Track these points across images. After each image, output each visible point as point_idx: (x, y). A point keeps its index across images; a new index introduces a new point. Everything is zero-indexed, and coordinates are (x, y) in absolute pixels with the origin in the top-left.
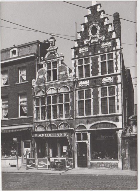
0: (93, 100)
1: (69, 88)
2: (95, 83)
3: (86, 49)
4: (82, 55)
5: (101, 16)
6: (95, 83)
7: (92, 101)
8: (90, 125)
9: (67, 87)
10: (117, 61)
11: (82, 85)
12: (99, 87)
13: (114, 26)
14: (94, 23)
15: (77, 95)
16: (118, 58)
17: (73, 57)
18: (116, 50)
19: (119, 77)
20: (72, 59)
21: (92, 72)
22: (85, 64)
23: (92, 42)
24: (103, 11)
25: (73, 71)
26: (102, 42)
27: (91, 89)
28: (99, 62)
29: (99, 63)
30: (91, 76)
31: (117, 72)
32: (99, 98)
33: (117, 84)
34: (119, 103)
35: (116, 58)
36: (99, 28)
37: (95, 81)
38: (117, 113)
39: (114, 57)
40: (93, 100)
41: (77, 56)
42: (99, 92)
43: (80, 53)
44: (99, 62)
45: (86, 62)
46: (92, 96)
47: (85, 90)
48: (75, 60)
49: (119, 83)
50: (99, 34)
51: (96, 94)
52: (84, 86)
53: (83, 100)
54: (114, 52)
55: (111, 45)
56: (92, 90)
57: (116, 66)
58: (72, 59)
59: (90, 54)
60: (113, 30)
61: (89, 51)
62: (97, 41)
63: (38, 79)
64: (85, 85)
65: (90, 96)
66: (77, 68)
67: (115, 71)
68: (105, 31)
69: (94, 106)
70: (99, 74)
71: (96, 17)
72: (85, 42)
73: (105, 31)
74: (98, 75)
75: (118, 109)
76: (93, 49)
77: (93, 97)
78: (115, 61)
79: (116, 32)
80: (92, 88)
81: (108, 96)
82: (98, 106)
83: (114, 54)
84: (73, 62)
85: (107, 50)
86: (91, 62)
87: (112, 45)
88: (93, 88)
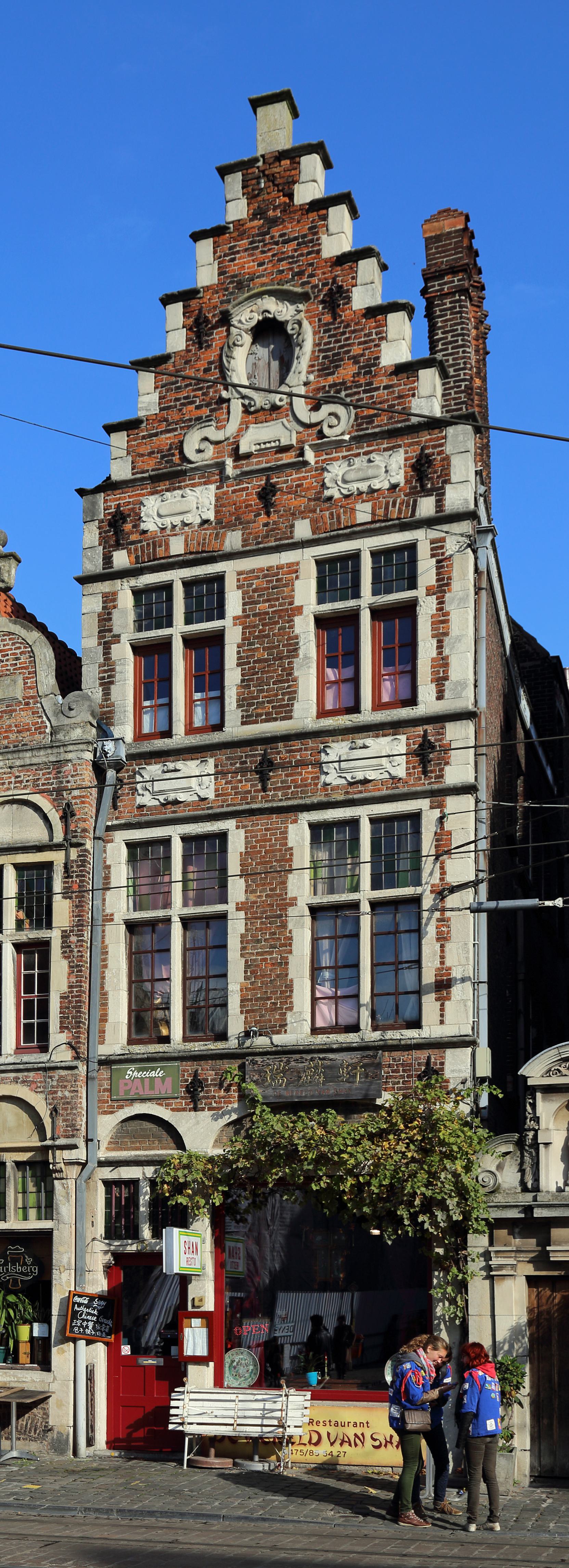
0: (242, 914)
2: (264, 780)
5: (324, 238)
6: (264, 780)
7: (236, 927)
10: (447, 607)
13: (430, 314)
14: (270, 293)
15: (121, 874)
16: (455, 585)
17: (94, 565)
18: (442, 519)
20: (84, 580)
21: (245, 683)
22: (188, 621)
24: (345, 199)
25: (90, 674)
27: (229, 825)
28: (299, 610)
29: (297, 620)
31: (440, 697)
33: (438, 795)
34: (448, 946)
36: (308, 330)
38: (431, 1030)
40: (242, 914)
44: (299, 610)
45: (200, 604)
47: (185, 839)
53: (160, 913)
54: (422, 537)
58: (84, 580)
59: (233, 540)
60: (426, 354)
65: (224, 886)
66: (123, 653)
67: (432, 688)
68: (355, 359)
69: (247, 966)
70: (295, 714)
71: (288, 248)
72: (192, 443)
73: (355, 359)
76: (254, 501)
78: (427, 608)
79: (444, 375)
81: (366, 894)
84: (92, 604)
85: (368, 518)
86: (239, 612)
87: (407, 481)
88: (248, 822)
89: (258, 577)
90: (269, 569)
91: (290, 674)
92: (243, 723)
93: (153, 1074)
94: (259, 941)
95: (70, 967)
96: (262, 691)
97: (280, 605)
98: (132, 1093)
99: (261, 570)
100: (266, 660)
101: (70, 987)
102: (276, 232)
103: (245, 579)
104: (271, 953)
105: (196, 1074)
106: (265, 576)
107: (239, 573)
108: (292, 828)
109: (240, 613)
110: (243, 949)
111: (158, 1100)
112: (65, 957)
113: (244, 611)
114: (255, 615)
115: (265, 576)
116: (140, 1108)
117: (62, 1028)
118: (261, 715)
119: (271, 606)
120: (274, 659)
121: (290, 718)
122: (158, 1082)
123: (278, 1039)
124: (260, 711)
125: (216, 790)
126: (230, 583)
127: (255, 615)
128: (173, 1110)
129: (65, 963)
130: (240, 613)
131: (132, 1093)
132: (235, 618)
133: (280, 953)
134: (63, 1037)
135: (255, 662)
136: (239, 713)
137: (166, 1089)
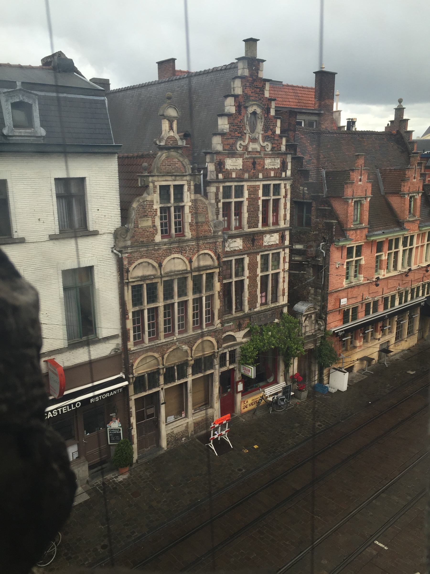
1: (215, 258)
3: (240, 161)
4: (230, 176)
8: (243, 333)
9: (209, 255)
11: (232, 247)
12: (257, 253)
19: (287, 233)
21: (249, 218)
23: (250, 149)
26: (267, 155)
27: (246, 256)
30: (246, 229)
32: (258, 276)
35: (285, 197)
37: (253, 240)
39: (283, 191)
41: (221, 176)
42: (258, 262)
43: (227, 169)
46: (247, 273)
48: (216, 185)
49: (287, 247)
50: (262, 134)
51: (253, 267)
52: (235, 250)
55: (279, 166)
56: (247, 261)
57: (285, 211)
61: (244, 170)
62: (259, 149)
63: (136, 229)
64: (237, 249)
69: (249, 293)
71: (258, 90)
74: (258, 227)
75: (283, 295)
77: (249, 273)
80: (248, 254)
82: (256, 291)
83: (282, 186)
89: (251, 188)
90: (254, 185)
91: (258, 216)
92: (248, 228)
93: (230, 324)
94: (251, 286)
95: (220, 301)
96: (252, 220)
97: (256, 196)
98: (226, 330)
99: (252, 186)
100: (253, 211)
101: (220, 307)
102: (255, 83)
103: (249, 187)
104: (253, 289)
105: (239, 322)
106: (253, 188)
107: (248, 186)
108: (258, 256)
109: (248, 197)
110: (248, 288)
111: (231, 331)
112: (219, 299)
113: (248, 197)
114: (251, 198)
115: (253, 188)
116: (228, 334)
117: (219, 319)
118: (252, 226)
119: (254, 196)
120: (255, 211)
121: (258, 227)
122: (231, 326)
123: (256, 310)
124: (252, 225)
125: (243, 247)
126: (245, 188)
127: (251, 198)
128: (234, 332)
129: (219, 300)
130: (248, 197)
131: (226, 330)
132: (247, 199)
133: (255, 288)
134: (219, 321)
135: (251, 211)
136: (247, 225)
137: (233, 327)
